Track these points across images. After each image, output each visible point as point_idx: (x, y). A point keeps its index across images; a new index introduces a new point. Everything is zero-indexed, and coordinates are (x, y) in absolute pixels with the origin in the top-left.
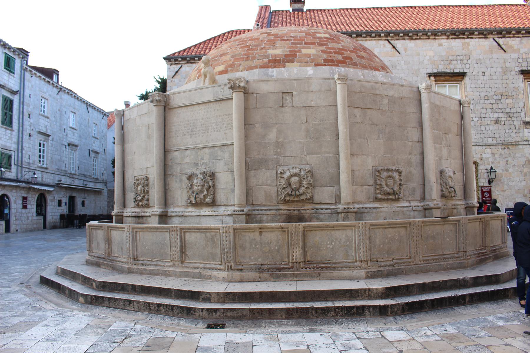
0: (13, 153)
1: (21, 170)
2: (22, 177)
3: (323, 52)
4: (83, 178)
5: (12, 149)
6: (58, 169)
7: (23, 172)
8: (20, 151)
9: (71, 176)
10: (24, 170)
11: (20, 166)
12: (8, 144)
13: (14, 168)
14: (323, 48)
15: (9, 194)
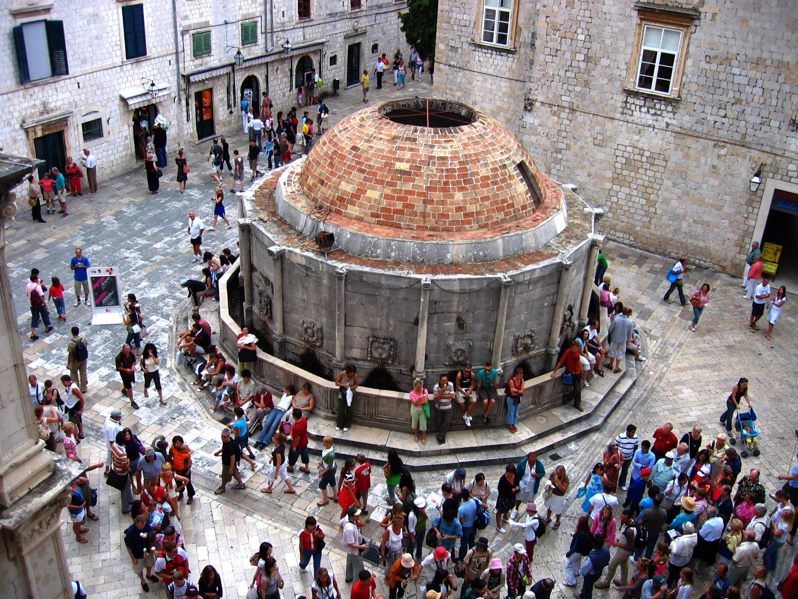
0: (259, 19)
1: (272, 37)
2: (273, 45)
3: (387, 197)
4: (375, 12)
5: (258, 14)
6: (331, 14)
7: (275, 38)
8: (268, 12)
9: (353, 16)
10: (275, 35)
11: (270, 32)
12: (251, 11)
13: (261, 38)
14: (388, 191)
15: (256, 74)
